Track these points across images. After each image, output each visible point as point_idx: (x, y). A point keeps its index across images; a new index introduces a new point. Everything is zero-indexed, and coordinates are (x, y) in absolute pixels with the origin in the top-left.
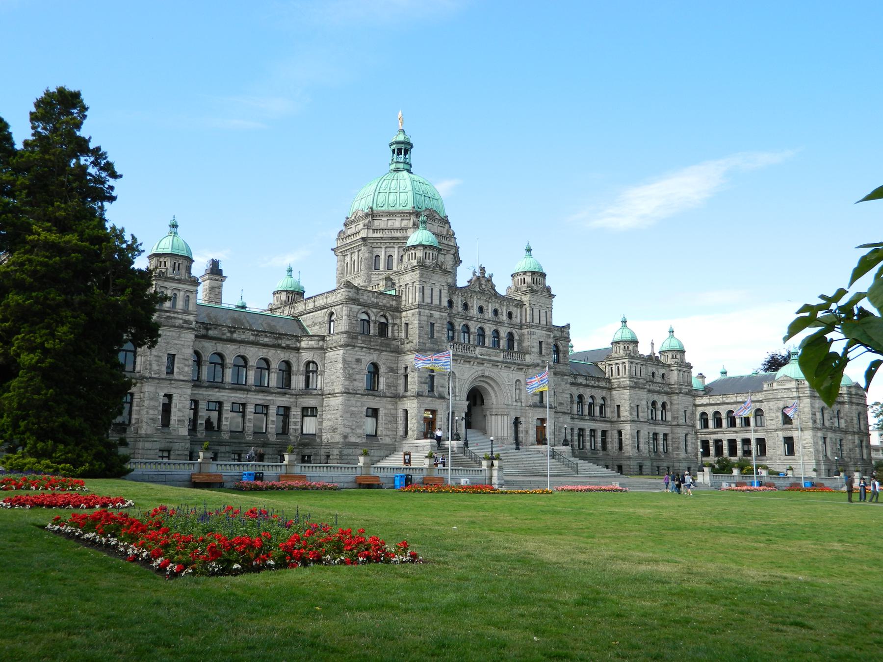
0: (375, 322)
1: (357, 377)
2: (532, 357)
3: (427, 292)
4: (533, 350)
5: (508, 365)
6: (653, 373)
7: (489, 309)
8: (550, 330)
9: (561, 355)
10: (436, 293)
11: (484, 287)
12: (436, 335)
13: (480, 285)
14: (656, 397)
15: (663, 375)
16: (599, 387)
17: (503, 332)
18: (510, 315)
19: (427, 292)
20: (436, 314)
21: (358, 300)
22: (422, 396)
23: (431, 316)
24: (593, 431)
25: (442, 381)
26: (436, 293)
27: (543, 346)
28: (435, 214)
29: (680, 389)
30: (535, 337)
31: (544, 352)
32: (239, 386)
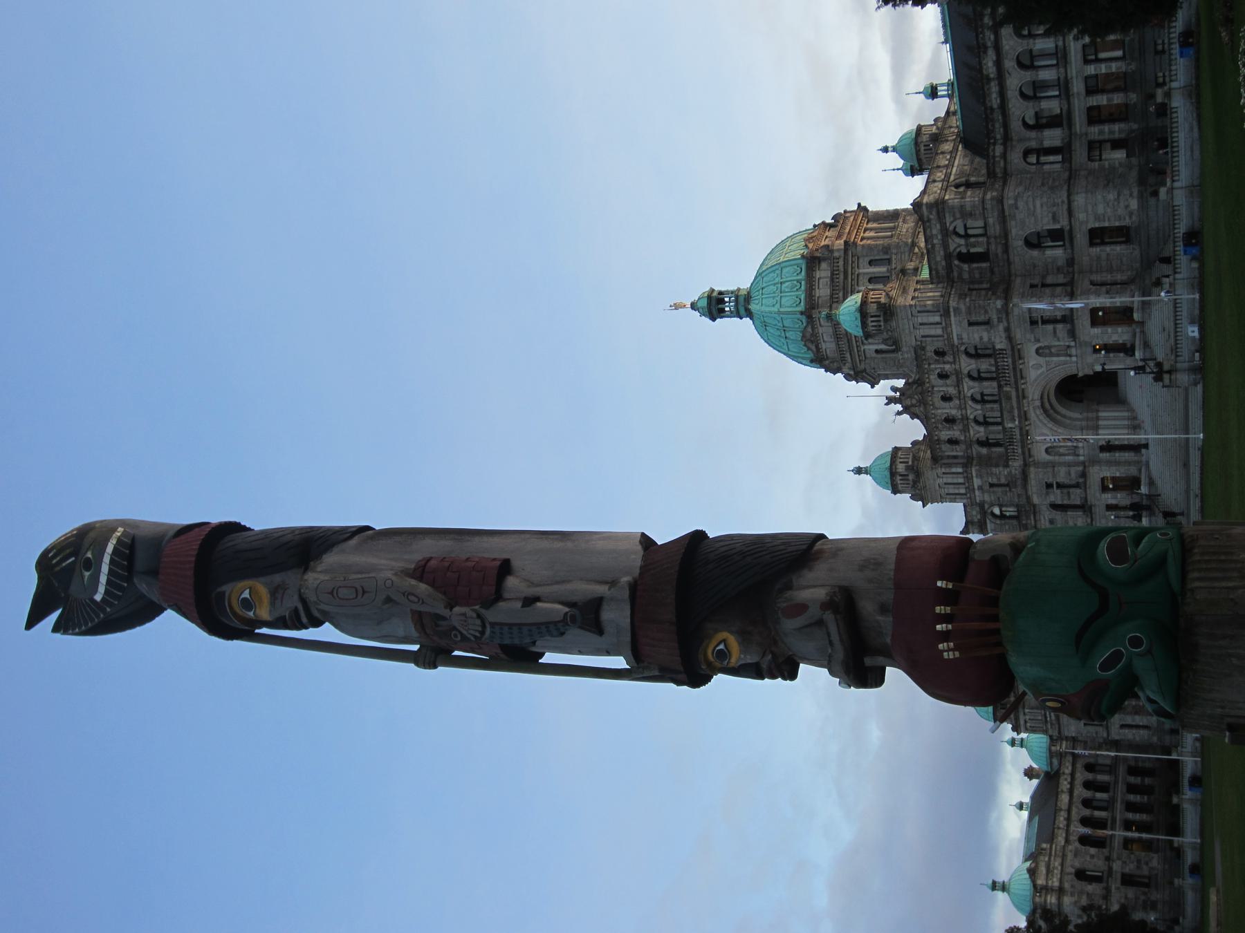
2: (997, 340)
4: (986, 339)
5: (1019, 375)
7: (941, 387)
8: (946, 314)
11: (914, 401)
12: (1003, 481)
17: (967, 365)
18: (940, 353)
20: (977, 482)
21: (979, 521)
22: (1086, 499)
23: (980, 488)
27: (974, 319)
28: (808, 335)
30: (965, 336)
31: (982, 318)
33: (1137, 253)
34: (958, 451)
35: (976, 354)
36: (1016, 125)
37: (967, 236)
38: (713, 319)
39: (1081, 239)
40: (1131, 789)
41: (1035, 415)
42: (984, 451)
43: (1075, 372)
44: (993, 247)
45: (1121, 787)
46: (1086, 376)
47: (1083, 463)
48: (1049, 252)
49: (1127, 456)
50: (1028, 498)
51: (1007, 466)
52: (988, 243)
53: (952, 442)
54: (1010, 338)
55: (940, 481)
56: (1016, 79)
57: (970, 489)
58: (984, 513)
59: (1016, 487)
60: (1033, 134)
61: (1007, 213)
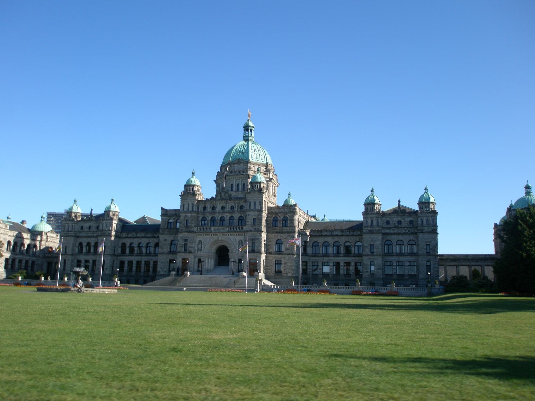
0: (174, 222)
1: (164, 247)
3: (186, 206)
4: (248, 223)
6: (400, 222)
9: (289, 222)
10: (191, 206)
12: (189, 224)
13: (221, 196)
14: (400, 237)
15: (411, 222)
16: (353, 235)
17: (236, 216)
18: (241, 207)
19: (186, 206)
20: (189, 215)
23: (186, 216)
24: (348, 264)
25: (191, 245)
26: (191, 206)
29: (422, 230)
31: (256, 223)
32: (140, 254)
33: (272, 275)
34: (201, 209)
35: (241, 219)
36: (315, 239)
37: (283, 220)
38: (244, 127)
39: (278, 257)
40: (27, 262)
41: (215, 238)
42: (200, 219)
43: (230, 251)
44: (278, 228)
45: (27, 258)
46: (228, 255)
47: (195, 253)
48: (274, 246)
49: (196, 267)
50: (182, 232)
51: (195, 226)
52: (280, 227)
53: (205, 208)
54: (248, 231)
55: (190, 202)
56: (330, 240)
57: (186, 212)
58: (171, 216)
59: (186, 229)
60: (311, 244)
61: (291, 234)
